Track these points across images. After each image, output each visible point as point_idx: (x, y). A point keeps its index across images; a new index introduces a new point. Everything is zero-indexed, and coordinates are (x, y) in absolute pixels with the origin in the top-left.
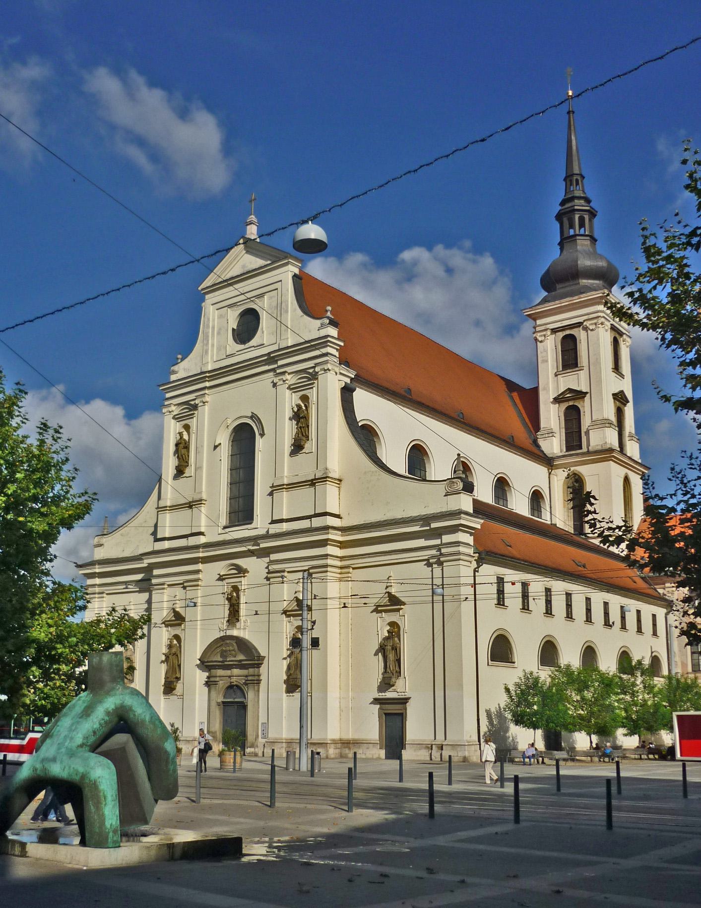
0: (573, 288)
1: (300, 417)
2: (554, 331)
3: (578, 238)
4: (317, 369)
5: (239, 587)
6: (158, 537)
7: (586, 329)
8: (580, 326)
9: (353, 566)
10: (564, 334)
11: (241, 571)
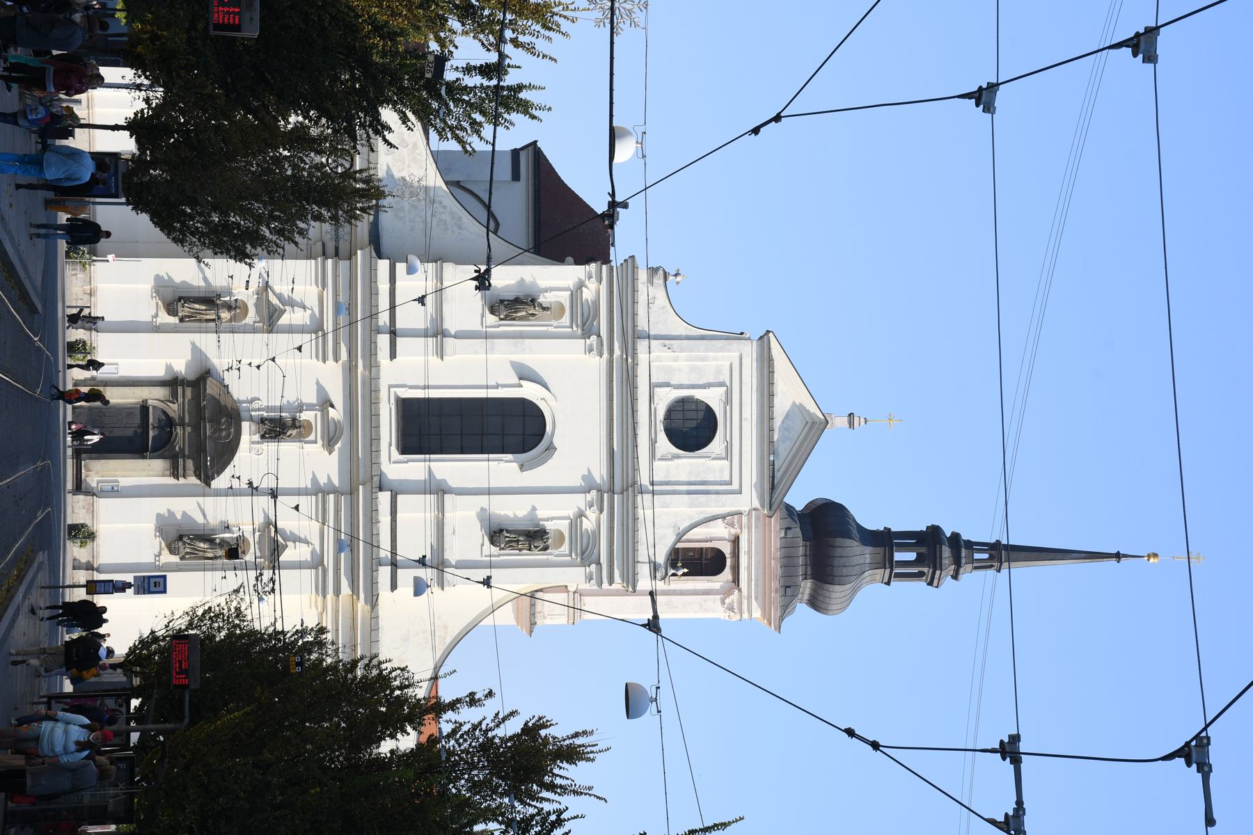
0: (801, 571)
1: (534, 537)
2: (736, 541)
3: (888, 571)
4: (593, 567)
5: (312, 437)
6: (397, 264)
7: (726, 593)
8: (734, 581)
9: (324, 614)
10: (727, 556)
11: (329, 444)
